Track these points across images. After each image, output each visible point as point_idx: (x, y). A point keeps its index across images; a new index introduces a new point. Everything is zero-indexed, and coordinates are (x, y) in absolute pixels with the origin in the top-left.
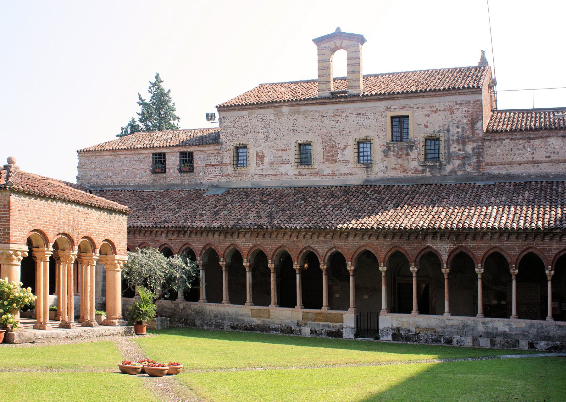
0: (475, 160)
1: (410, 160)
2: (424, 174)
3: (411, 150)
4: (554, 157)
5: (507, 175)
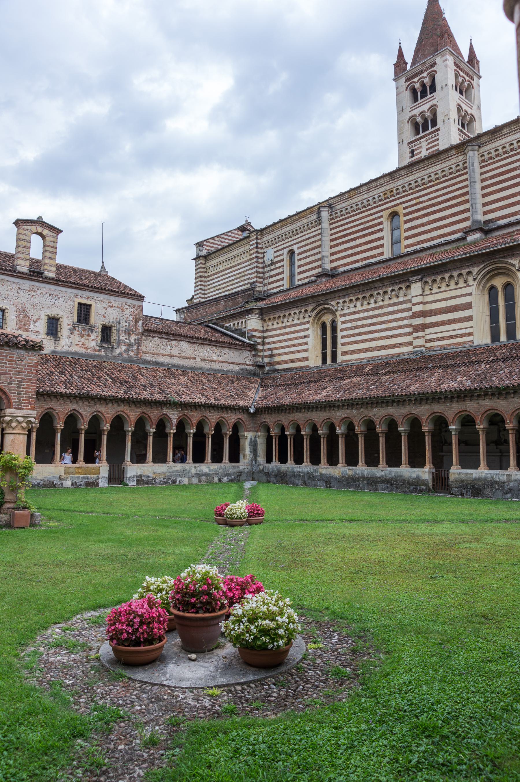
0: (136, 348)
1: (90, 340)
2: (100, 353)
3: (92, 332)
4: (183, 354)
5: (155, 361)
